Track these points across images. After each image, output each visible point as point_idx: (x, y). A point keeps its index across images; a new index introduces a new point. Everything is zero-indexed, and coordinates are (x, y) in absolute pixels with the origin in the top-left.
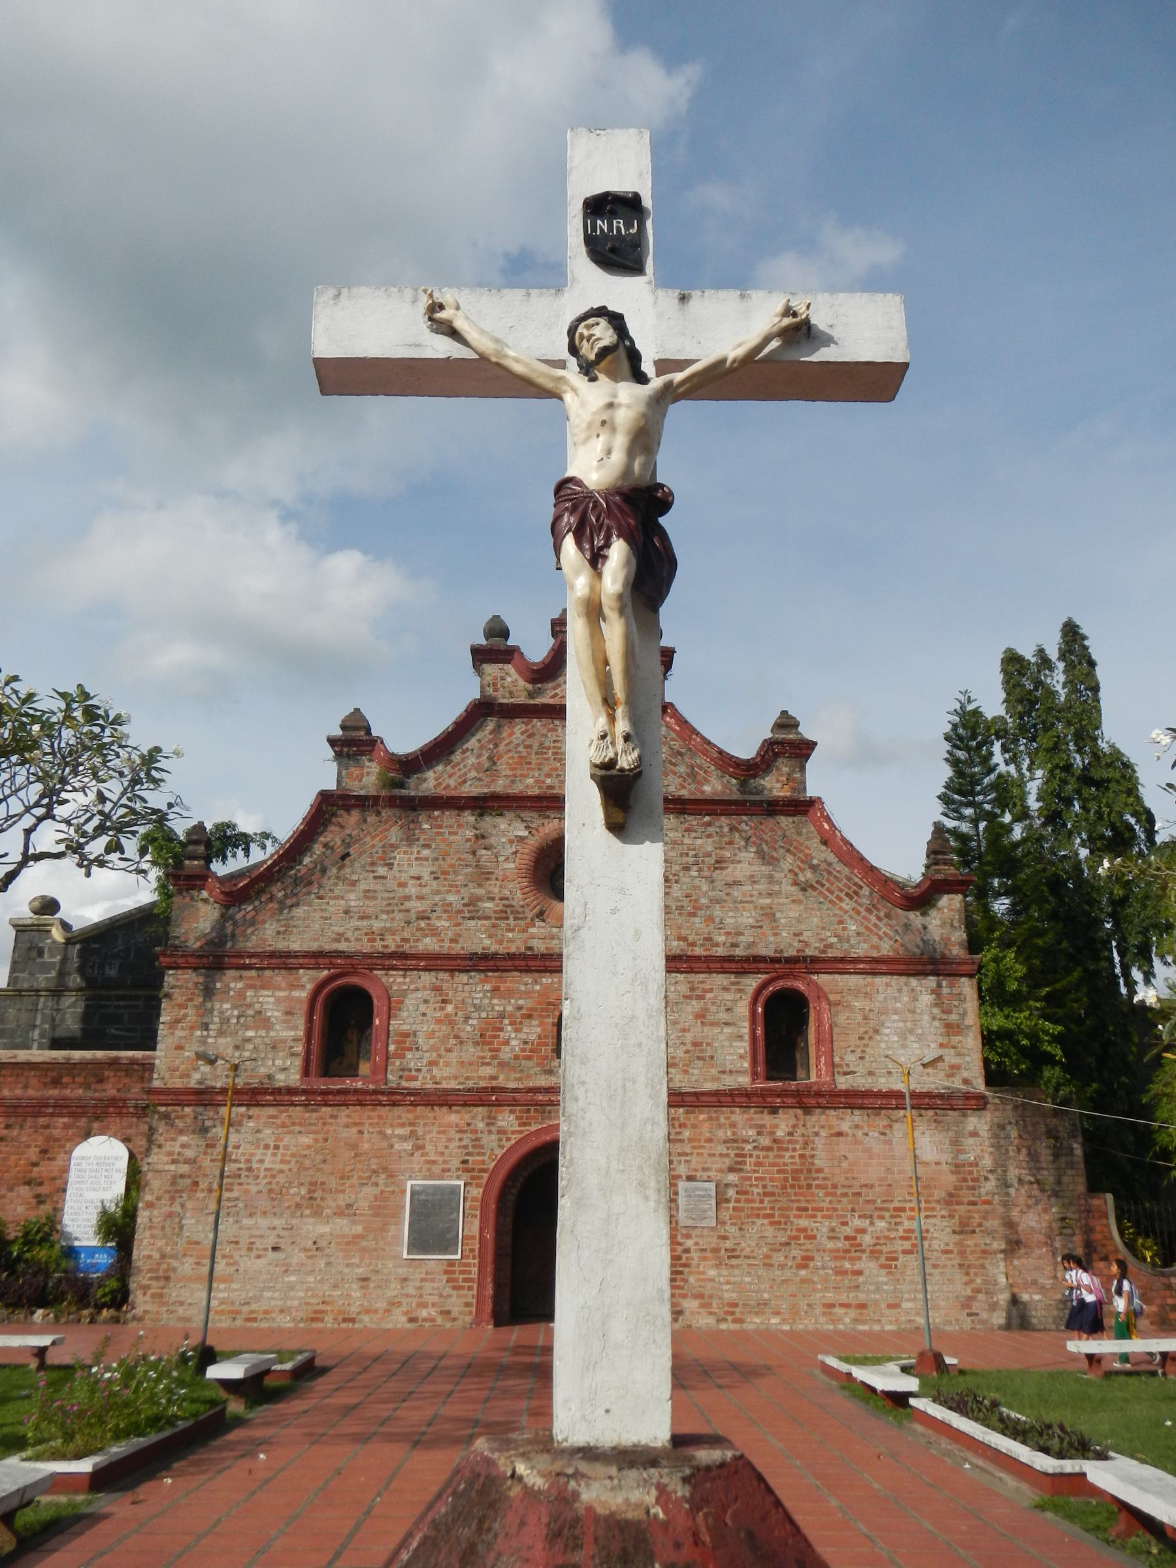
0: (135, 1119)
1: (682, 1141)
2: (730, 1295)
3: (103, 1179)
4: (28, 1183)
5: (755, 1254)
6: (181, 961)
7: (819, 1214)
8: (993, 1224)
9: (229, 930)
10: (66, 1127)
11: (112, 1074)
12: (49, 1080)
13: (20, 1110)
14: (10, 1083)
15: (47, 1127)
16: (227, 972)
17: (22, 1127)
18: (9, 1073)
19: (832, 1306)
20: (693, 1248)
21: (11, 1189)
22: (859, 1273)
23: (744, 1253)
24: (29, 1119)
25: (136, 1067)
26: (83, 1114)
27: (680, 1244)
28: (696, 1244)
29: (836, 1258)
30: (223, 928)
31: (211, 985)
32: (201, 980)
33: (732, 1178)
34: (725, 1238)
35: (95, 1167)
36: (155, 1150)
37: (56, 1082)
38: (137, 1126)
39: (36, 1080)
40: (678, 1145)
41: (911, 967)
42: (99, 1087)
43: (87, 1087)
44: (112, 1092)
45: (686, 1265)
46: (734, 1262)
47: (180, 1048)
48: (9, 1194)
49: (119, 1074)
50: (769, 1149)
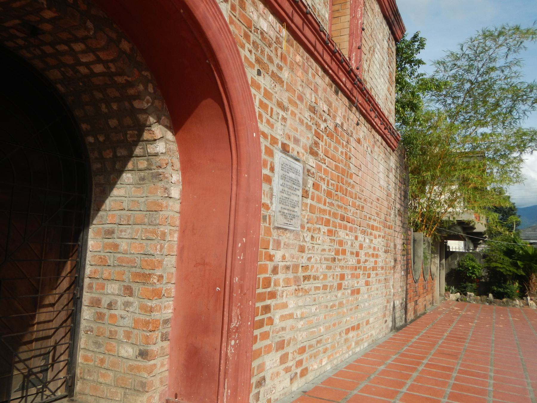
1: (280, 81)
2: (301, 337)
5: (318, 274)
7: (349, 225)
8: (392, 245)
19: (347, 331)
20: (281, 264)
22: (358, 291)
23: (312, 273)
27: (270, 258)
28: (284, 257)
29: (353, 276)
33: (312, 161)
34: (302, 249)
40: (278, 87)
41: (389, 9)
45: (273, 295)
46: (306, 285)
50: (330, 136)
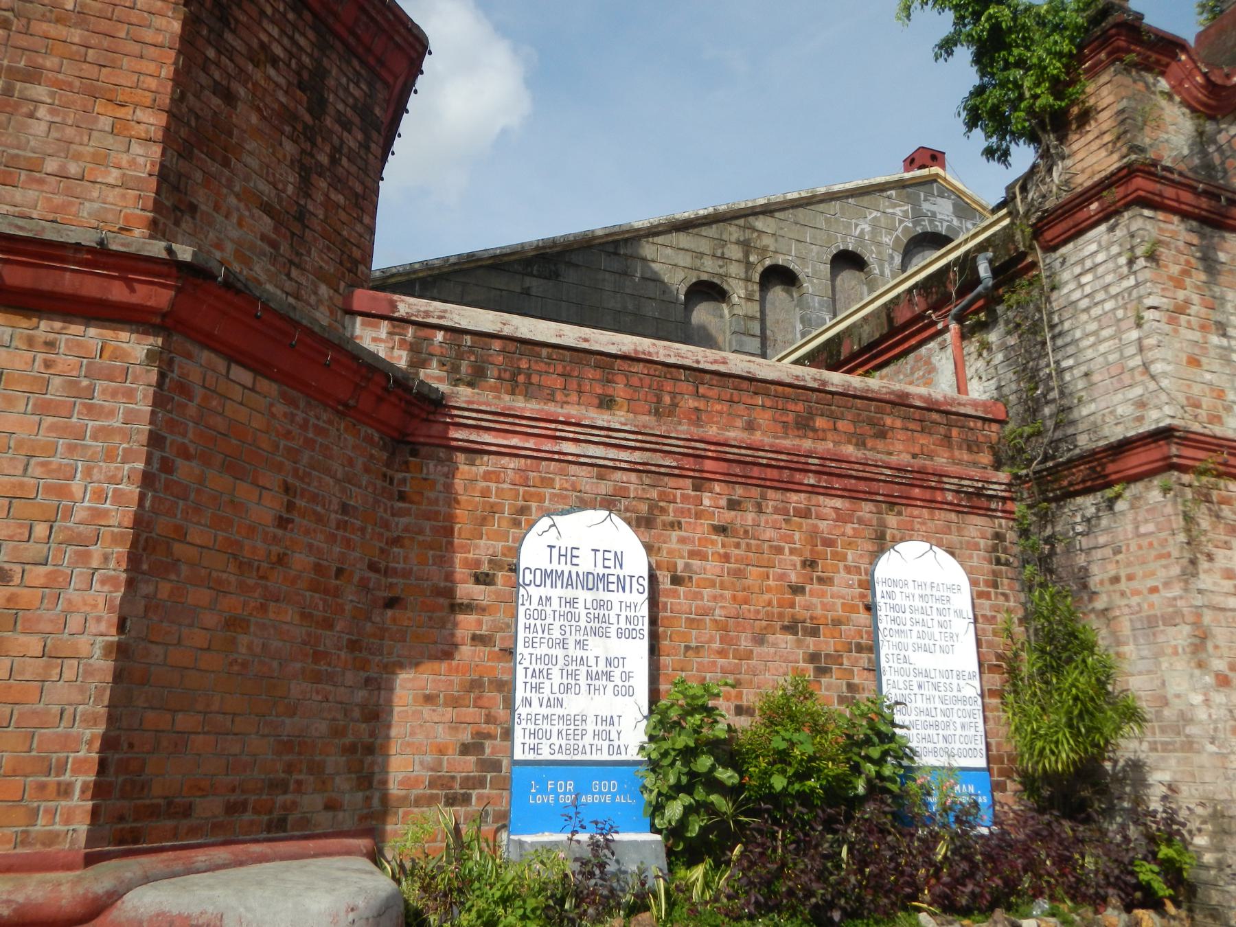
0: (953, 516)
3: (936, 630)
4: (791, 629)
6: (1169, 192)
9: (1217, 159)
10: (841, 518)
11: (898, 423)
12: (790, 418)
13: (756, 471)
14: (720, 413)
15: (805, 514)
16: (1227, 235)
17: (760, 509)
18: (714, 392)
21: (760, 640)
24: (771, 494)
25: (935, 416)
26: (868, 496)
30: (1204, 153)
31: (1211, 254)
32: (1195, 240)
35: (918, 603)
36: (1204, 564)
37: (804, 425)
38: (959, 529)
39: (768, 414)
42: (880, 444)
43: (861, 444)
44: (904, 459)
47: (1194, 362)
48: (757, 650)
49: (912, 426)
